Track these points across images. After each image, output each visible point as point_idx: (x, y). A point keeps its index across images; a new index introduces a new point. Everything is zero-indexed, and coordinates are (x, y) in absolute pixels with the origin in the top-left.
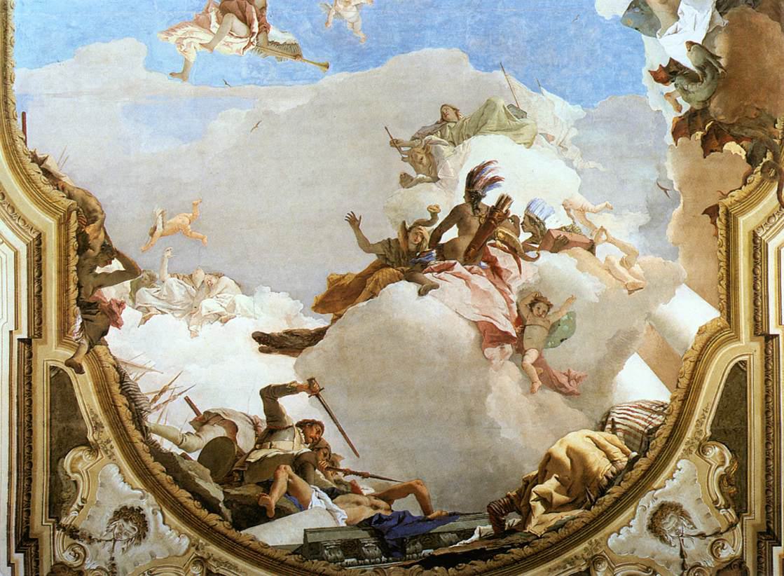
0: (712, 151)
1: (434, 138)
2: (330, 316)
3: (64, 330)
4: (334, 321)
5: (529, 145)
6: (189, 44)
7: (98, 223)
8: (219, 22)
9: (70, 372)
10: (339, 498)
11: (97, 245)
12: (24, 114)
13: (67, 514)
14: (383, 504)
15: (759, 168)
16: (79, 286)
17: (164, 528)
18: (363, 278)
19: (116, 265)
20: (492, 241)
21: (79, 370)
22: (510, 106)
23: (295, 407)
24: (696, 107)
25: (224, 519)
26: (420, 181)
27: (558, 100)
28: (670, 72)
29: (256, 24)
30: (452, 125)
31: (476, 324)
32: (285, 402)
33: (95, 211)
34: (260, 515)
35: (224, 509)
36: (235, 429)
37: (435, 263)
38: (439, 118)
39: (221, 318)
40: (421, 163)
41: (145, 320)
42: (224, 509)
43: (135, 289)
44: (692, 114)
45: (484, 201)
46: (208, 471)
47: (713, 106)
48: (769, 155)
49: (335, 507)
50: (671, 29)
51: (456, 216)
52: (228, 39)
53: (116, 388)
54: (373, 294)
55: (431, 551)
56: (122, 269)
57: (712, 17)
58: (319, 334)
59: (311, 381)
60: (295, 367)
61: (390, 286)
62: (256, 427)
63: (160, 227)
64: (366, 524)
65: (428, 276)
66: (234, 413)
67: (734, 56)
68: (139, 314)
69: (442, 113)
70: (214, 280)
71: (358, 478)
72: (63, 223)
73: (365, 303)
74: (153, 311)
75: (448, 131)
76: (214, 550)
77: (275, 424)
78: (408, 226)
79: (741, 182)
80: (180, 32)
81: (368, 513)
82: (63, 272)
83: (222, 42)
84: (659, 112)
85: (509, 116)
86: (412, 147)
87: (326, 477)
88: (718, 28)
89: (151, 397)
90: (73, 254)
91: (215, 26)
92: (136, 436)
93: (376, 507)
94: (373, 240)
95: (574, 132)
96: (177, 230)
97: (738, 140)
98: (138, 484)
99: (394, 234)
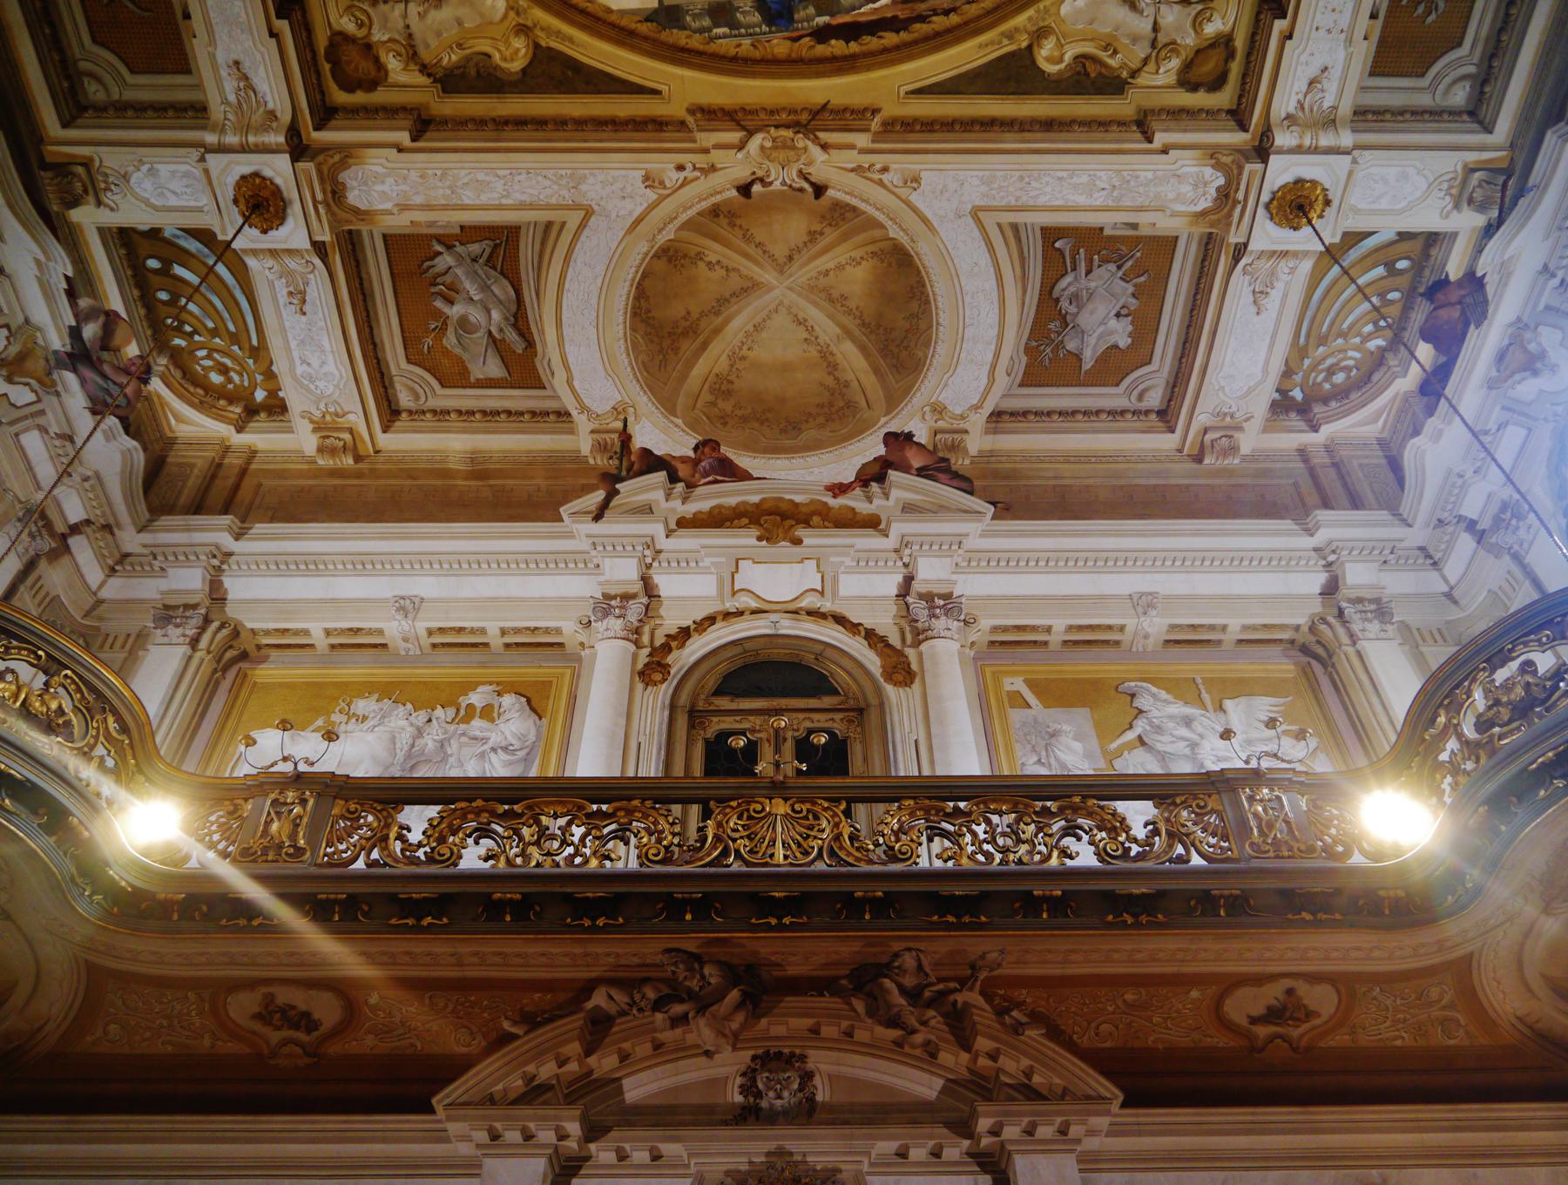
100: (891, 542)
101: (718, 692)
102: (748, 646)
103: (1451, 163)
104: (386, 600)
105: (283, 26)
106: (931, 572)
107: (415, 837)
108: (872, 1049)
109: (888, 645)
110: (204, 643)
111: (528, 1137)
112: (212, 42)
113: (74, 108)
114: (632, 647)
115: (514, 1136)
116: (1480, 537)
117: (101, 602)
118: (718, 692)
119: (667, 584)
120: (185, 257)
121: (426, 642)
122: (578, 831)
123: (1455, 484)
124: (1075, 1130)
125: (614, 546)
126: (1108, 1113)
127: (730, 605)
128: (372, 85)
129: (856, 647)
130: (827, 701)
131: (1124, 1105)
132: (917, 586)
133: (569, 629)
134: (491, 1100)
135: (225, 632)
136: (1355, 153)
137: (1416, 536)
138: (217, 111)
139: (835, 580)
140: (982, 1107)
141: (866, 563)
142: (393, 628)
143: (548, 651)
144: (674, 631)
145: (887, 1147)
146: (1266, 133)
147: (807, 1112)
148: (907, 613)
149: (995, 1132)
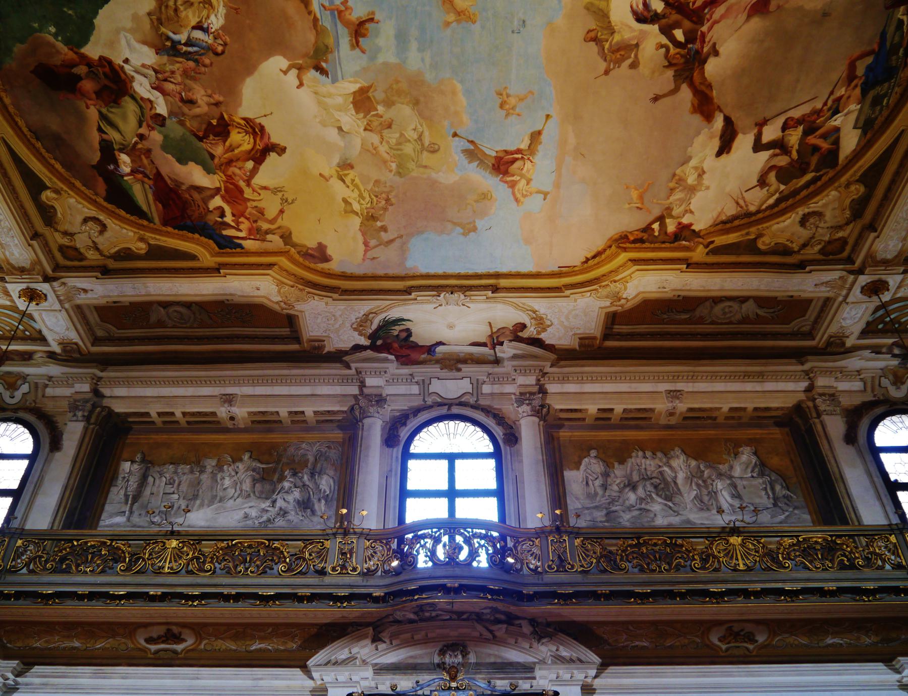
1: (607, 46)
2: (717, 113)
3: (687, 249)
4: (721, 111)
6: (527, 191)
7: (628, 234)
8: (513, 175)
9: (711, 246)
10: (840, 109)
11: (640, 235)
13: (793, 248)
14: (855, 82)
16: (664, 242)
17: (820, 203)
18: (696, 92)
19: (656, 226)
20: (691, 4)
21: (712, 242)
23: (771, 133)
25: (827, 172)
26: (636, 56)
29: (516, 156)
30: (599, 34)
31: (749, 16)
32: (766, 139)
33: (621, 236)
34: (834, 152)
35: (821, 173)
36: (772, 168)
37: (697, 45)
38: (593, 44)
39: (701, 174)
40: (623, 56)
41: (691, 212)
42: (821, 173)
43: (672, 217)
45: (659, 11)
46: (794, 181)
49: (845, 111)
51: (666, 31)
52: (525, 169)
53: (728, 226)
54: (710, 86)
55: (901, 51)
56: (658, 223)
58: (728, 121)
59: (756, 125)
60: (744, 133)
61: (706, 75)
62: (775, 155)
63: (638, 205)
64: (864, 93)
65: (705, 50)
66: (764, 166)
68: (687, 215)
69: (590, 41)
70: (677, 178)
71: (832, 97)
72: (625, 250)
73: (714, 92)
74: (688, 208)
75: (603, 37)
76: (843, 179)
77: (780, 145)
78: (667, 64)
80: (518, 196)
81: (858, 91)
82: (654, 250)
83: (526, 174)
87: (823, 116)
89: (739, 209)
90: (644, 246)
91: (516, 178)
92: (760, 215)
93: (856, 86)
94: (672, 86)
96: (641, 197)
98: (788, 215)
99: (670, 73)
103: (73, 336)
136: (63, 310)
146: (55, 279)
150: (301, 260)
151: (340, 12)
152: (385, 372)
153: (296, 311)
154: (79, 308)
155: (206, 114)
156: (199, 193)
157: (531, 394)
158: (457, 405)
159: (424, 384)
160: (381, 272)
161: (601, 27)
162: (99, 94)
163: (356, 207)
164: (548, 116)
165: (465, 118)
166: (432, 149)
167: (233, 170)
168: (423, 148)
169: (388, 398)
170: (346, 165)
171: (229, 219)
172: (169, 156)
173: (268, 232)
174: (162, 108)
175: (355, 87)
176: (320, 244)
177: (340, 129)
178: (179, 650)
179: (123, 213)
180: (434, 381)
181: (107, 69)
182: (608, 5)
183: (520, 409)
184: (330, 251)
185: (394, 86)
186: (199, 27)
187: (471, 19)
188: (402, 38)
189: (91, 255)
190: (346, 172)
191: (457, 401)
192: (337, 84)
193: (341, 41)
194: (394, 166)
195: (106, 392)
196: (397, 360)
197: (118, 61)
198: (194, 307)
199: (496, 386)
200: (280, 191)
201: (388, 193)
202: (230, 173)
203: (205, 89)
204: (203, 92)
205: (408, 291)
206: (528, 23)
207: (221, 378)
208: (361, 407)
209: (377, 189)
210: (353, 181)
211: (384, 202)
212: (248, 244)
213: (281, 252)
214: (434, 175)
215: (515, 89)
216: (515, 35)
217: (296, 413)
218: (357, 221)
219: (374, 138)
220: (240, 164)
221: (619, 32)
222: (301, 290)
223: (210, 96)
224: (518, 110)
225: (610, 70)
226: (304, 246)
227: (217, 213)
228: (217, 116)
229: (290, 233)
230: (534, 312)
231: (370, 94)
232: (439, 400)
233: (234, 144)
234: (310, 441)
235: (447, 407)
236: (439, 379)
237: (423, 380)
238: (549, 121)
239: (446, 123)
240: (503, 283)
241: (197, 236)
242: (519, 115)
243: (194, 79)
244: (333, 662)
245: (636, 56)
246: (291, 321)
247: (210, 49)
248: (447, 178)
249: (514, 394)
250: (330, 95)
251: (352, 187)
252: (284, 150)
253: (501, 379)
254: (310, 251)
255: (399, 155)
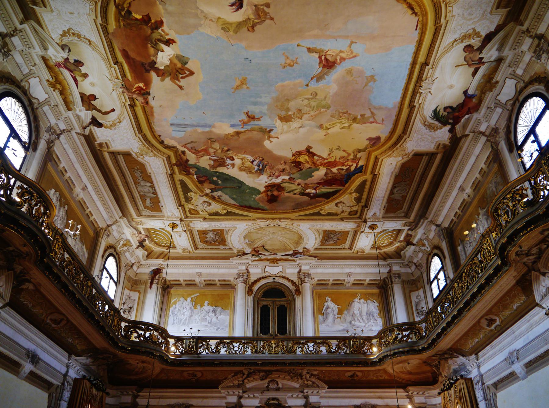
0: (146, 16)
1: (257, 21)
5: (219, 18)
8: (336, 59)
12: (416, 30)
15: (126, 9)
22: (228, 32)
24: (155, 31)
26: (262, 5)
27: (209, 33)
28: (169, 42)
30: (250, 25)
38: (255, 28)
44: (157, 28)
47: (149, 32)
48: (123, 13)
50: (171, 56)
57: (157, 59)
67: (146, 48)
69: (254, 29)
75: (251, 23)
79: (132, 4)
80: (351, 56)
84: (170, 29)
85: (228, 28)
86: (265, 18)
88: (154, 56)
91: (338, 58)
95: (202, 22)
97: (137, 19)
100: (297, 263)
101: (262, 297)
102: (268, 284)
104: (195, 273)
105: (180, 208)
106: (305, 268)
107: (213, 348)
108: (288, 380)
109: (296, 284)
110: (160, 283)
111: (234, 393)
112: (166, 208)
113: (140, 215)
114: (245, 285)
115: (231, 393)
116: (416, 266)
117: (137, 274)
118: (262, 297)
119: (251, 270)
120: (158, 231)
121: (204, 283)
122: (241, 346)
123: (411, 257)
124: (320, 392)
125: (241, 264)
126: (325, 389)
127: (264, 275)
128: (197, 214)
129: (289, 284)
130: (284, 299)
131: (328, 388)
132: (302, 271)
133: (233, 281)
134: (228, 387)
135: (163, 280)
137: (406, 262)
138: (166, 215)
139: (285, 270)
140: (305, 389)
141: (292, 267)
142: (197, 280)
143: (228, 286)
144: (253, 281)
145: (291, 394)
147: (278, 389)
148: (299, 278)
149: (307, 392)
150: (376, 147)
151: (244, 123)
152: (479, 120)
153: (411, 152)
154: (383, 218)
155: (290, 166)
156: (328, 174)
157: (538, 46)
158: (519, 95)
159: (498, 104)
160: (394, 118)
161: (246, 25)
162: (279, 191)
163: (346, 125)
164: (298, 45)
165: (297, 81)
166: (315, 95)
167: (318, 162)
168: (314, 98)
169: (497, 126)
170: (321, 127)
171: (345, 168)
172: (309, 179)
173: (355, 156)
174: (287, 178)
175: (279, 122)
176: (367, 140)
177: (300, 127)
178: (499, 324)
179: (335, 196)
180: (498, 98)
181: (269, 187)
182: (234, 23)
183: (543, 61)
184: (374, 136)
185: (279, 107)
186: (252, 162)
187: (245, 79)
188: (255, 104)
189: (355, 208)
190: (325, 127)
191: (518, 93)
192: (277, 126)
193: (257, 124)
194: (322, 110)
195: (439, 223)
196: (471, 113)
197: (266, 184)
198: (396, 185)
199: (520, 65)
200: (332, 150)
201: (339, 113)
202: (320, 164)
203: (278, 165)
204: (280, 166)
205: (412, 107)
206: (246, 57)
207: (450, 185)
208: (494, 142)
209: (337, 117)
210: (330, 125)
211: (345, 115)
212: (361, 163)
213: (369, 154)
214: (331, 94)
215: (282, 60)
216: (252, 62)
217: (480, 171)
218: (355, 125)
219: (306, 116)
220: (315, 161)
221: (248, 16)
222: (397, 149)
223: (281, 164)
224: (294, 59)
225: (270, 17)
226: (367, 145)
227: (340, 171)
228: (291, 164)
229: (358, 149)
230: (456, 41)
231: (283, 116)
232: (512, 102)
233: (305, 161)
234: (490, 181)
235: (517, 101)
236: (498, 95)
237: (495, 103)
238: (301, 44)
239: (300, 89)
240: (421, 59)
241: (352, 178)
242: (297, 59)
243: (274, 167)
244: (543, 295)
245: (262, 5)
246: (418, 155)
247: (261, 161)
248: (333, 88)
249: (532, 57)
250: (283, 129)
251: (334, 126)
252: (309, 146)
253: (517, 60)
254: (371, 143)
255: (317, 107)
